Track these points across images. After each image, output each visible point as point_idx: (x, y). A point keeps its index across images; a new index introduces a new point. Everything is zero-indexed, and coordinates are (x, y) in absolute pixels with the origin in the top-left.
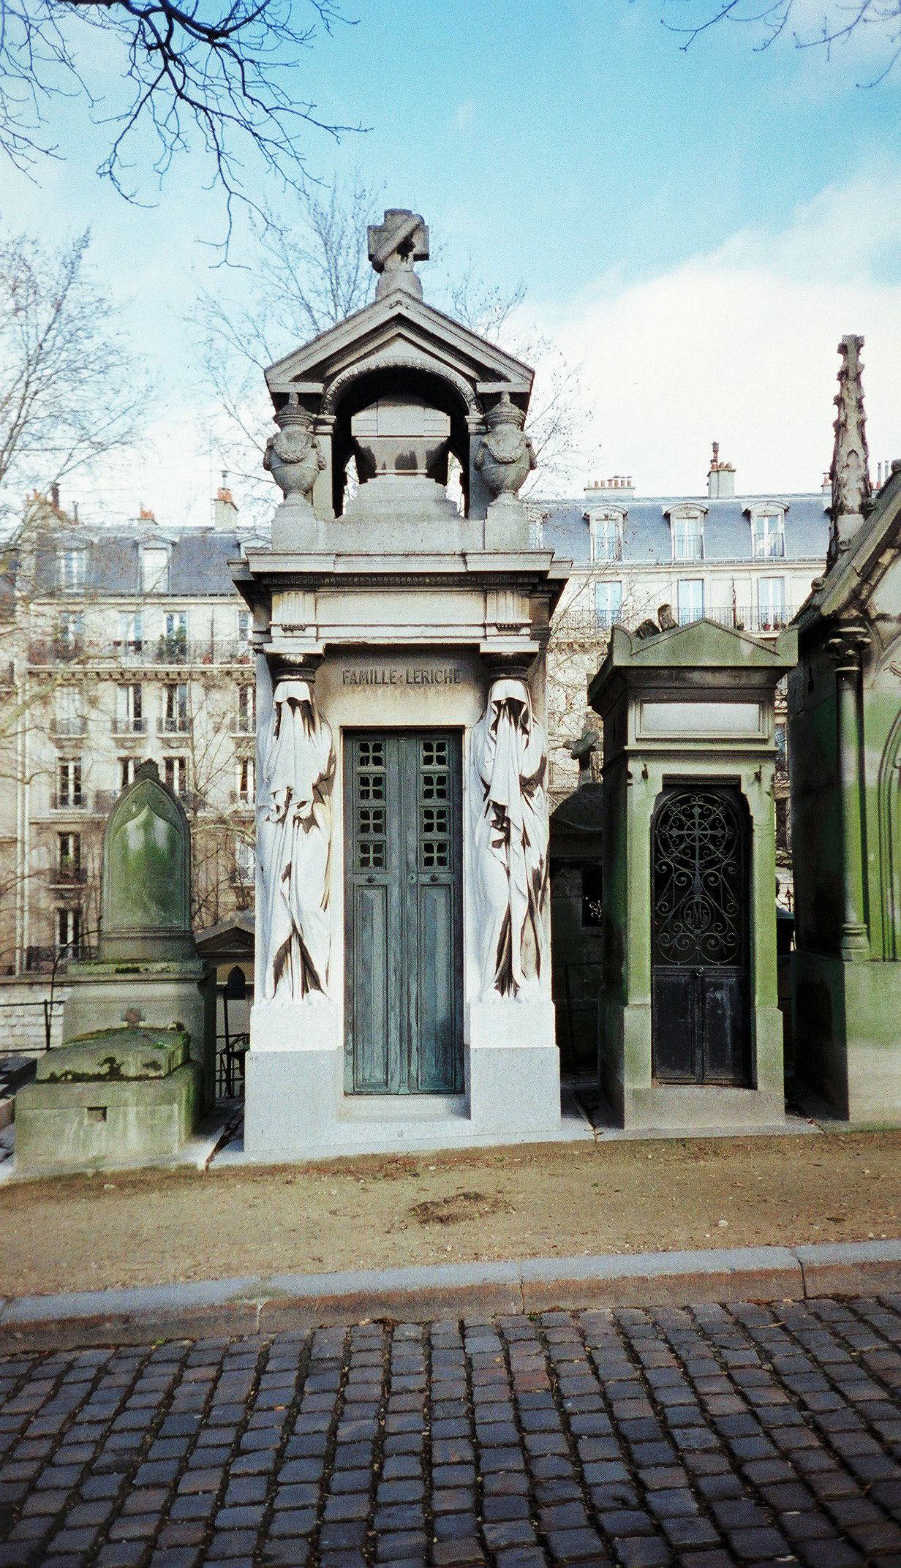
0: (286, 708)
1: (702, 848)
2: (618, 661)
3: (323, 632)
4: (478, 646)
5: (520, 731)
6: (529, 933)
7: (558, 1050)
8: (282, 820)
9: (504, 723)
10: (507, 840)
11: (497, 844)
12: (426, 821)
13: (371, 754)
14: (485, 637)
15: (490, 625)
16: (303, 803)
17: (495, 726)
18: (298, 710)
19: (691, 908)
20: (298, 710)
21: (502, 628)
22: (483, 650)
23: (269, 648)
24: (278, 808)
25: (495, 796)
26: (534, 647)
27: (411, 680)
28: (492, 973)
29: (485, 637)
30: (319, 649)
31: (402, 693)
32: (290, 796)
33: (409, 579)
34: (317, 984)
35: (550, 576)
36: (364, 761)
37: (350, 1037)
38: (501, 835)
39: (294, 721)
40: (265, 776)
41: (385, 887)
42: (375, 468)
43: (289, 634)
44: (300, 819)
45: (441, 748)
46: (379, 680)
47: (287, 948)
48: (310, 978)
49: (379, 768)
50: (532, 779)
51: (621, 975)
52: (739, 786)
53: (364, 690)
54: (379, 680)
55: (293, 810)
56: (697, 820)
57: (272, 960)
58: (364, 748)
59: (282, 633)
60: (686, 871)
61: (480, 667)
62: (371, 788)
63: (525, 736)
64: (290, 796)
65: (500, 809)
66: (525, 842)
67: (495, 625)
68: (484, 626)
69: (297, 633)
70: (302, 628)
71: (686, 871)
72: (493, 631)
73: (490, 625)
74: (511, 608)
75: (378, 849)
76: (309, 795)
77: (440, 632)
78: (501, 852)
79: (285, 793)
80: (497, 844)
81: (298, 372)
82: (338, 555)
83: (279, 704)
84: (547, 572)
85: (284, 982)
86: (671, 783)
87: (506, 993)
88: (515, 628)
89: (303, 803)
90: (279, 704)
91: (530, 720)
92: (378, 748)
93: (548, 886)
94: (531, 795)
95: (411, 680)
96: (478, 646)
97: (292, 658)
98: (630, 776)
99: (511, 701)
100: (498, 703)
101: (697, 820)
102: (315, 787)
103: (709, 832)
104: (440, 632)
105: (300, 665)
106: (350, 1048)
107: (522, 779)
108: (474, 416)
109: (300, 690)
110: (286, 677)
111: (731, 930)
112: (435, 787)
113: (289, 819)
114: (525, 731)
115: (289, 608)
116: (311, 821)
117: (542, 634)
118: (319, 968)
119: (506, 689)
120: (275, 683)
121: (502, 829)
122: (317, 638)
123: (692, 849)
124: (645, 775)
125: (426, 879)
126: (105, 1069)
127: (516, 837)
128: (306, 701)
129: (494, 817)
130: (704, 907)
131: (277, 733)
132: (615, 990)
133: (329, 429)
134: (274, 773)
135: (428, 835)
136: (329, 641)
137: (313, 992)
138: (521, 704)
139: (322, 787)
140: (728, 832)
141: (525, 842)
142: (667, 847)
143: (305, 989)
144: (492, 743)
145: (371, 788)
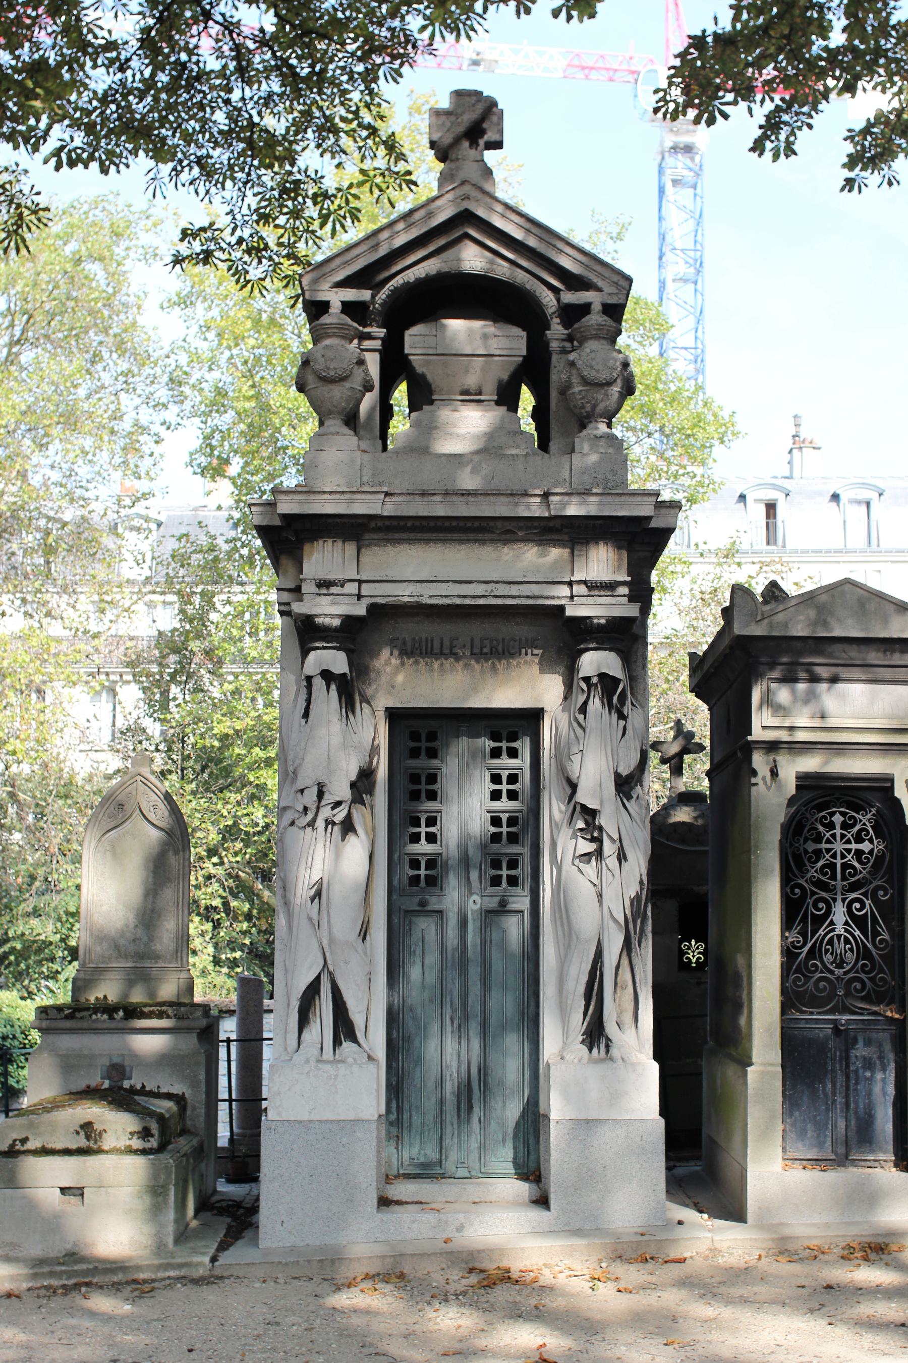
1: (845, 866)
2: (739, 629)
3: (366, 589)
4: (562, 608)
5: (615, 716)
7: (662, 1122)
8: (312, 824)
9: (595, 704)
10: (599, 853)
13: (424, 745)
14: (572, 597)
16: (338, 804)
17: (583, 709)
18: (333, 687)
19: (831, 942)
20: (333, 687)
21: (592, 586)
22: (569, 612)
23: (297, 608)
24: (306, 809)
25: (582, 797)
26: (633, 611)
27: (476, 651)
29: (572, 597)
32: (320, 795)
33: (476, 524)
34: (355, 1040)
35: (653, 524)
36: (415, 753)
37: (394, 1105)
38: (590, 847)
39: (327, 701)
40: (291, 769)
41: (440, 912)
42: (431, 392)
43: (324, 591)
44: (334, 824)
45: (513, 737)
46: (436, 649)
47: (313, 989)
48: (344, 1028)
50: (630, 776)
51: (736, 1028)
52: (892, 788)
54: (436, 649)
55: (326, 812)
56: (838, 831)
57: (295, 1004)
58: (415, 736)
59: (315, 590)
60: (824, 894)
61: (563, 638)
62: (423, 787)
63: (622, 723)
64: (320, 795)
65: (590, 814)
66: (622, 857)
67: (585, 582)
68: (570, 584)
69: (334, 590)
71: (824, 894)
72: (583, 589)
73: (579, 582)
74: (602, 562)
76: (345, 793)
77: (514, 590)
78: (590, 870)
79: (315, 789)
81: (340, 276)
82: (387, 494)
83: (309, 679)
84: (649, 519)
85: (312, 1034)
86: (806, 782)
87: (595, 1050)
88: (610, 587)
89: (338, 804)
91: (628, 703)
92: (432, 736)
93: (649, 913)
94: (629, 798)
95: (476, 651)
96: (562, 608)
97: (327, 621)
98: (754, 773)
99: (602, 676)
100: (587, 679)
101: (838, 831)
102: (353, 785)
103: (854, 846)
104: (514, 590)
105: (336, 630)
106: (393, 1117)
107: (617, 775)
108: (556, 330)
109: (338, 662)
110: (320, 644)
111: (881, 971)
112: (504, 787)
113: (320, 823)
114: (622, 716)
115: (324, 559)
116: (348, 827)
117: (642, 593)
118: (357, 1018)
119: (594, 661)
120: (305, 653)
121: (593, 839)
122: (359, 597)
123: (832, 866)
124: (774, 773)
126: (82, 1142)
127: (609, 848)
128: (345, 674)
129: (581, 824)
130: (847, 941)
131: (306, 715)
132: (733, 1045)
133: (377, 344)
134: (300, 765)
136: (374, 600)
137: (347, 1046)
138: (616, 681)
139: (363, 783)
140: (878, 846)
141: (622, 857)
142: (800, 865)
143: (337, 1042)
144: (579, 731)
145: (423, 787)
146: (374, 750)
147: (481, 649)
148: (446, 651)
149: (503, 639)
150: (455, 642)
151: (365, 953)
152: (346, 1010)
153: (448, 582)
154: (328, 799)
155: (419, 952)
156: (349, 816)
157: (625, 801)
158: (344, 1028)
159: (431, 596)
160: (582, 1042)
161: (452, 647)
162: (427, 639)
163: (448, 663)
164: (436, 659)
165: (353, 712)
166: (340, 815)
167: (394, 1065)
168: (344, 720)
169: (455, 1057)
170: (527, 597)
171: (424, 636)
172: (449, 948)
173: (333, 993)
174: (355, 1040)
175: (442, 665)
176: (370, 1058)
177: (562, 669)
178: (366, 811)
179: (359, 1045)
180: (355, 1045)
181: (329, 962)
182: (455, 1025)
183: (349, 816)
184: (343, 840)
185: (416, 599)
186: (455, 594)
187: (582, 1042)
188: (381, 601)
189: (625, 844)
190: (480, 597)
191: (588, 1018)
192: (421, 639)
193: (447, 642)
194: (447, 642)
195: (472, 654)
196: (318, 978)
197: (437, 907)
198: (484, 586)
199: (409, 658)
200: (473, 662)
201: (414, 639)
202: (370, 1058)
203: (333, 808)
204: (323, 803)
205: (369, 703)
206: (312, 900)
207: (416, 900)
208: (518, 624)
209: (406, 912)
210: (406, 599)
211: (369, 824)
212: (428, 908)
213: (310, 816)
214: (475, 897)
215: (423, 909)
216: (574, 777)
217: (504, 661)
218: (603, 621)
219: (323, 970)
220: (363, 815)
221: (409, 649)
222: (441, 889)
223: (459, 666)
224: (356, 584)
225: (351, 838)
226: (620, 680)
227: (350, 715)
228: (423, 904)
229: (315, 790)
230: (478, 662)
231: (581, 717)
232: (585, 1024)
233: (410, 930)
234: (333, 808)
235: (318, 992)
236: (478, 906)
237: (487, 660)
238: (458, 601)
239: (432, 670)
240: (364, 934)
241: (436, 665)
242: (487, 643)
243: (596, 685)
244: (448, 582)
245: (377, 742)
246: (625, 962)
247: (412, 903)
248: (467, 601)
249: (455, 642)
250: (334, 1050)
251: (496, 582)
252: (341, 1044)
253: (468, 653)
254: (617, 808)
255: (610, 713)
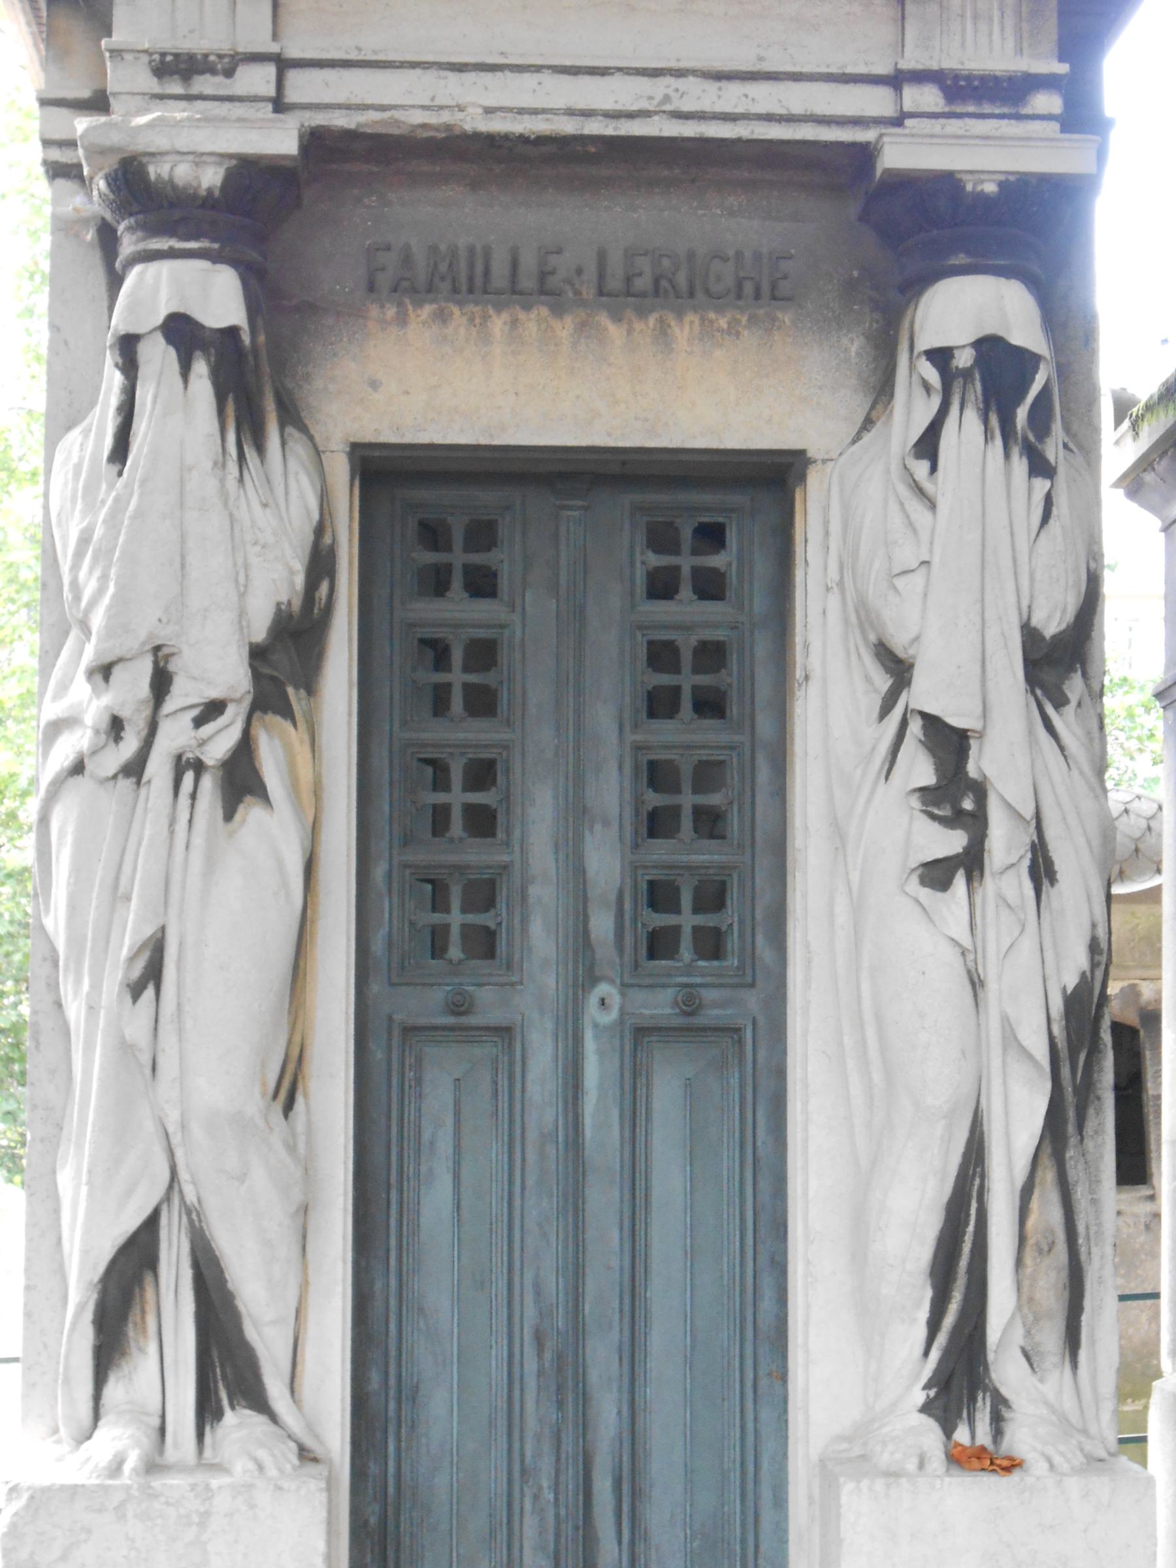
0: (157, 356)
3: (301, 86)
4: (865, 154)
5: (1020, 465)
6: (1047, 1211)
8: (135, 769)
9: (965, 433)
10: (972, 862)
11: (937, 874)
12: (654, 799)
15: (920, 77)
16: (213, 709)
17: (928, 445)
20: (201, 368)
27: (615, 283)
28: (907, 1358)
30: (281, 141)
31: (582, 326)
32: (161, 683)
34: (259, 1403)
38: (953, 842)
39: (182, 411)
41: (504, 1033)
43: (177, 88)
44: (199, 767)
48: (228, 1371)
49: (481, 610)
53: (442, 317)
55: (177, 733)
58: (433, 534)
64: (161, 683)
65: (949, 743)
66: (1042, 870)
70: (231, 64)
72: (927, 97)
73: (920, 77)
75: (484, 893)
77: (732, 97)
80: (937, 874)
89: (213, 709)
90: (128, 346)
92: (483, 534)
94: (1060, 702)
100: (941, 357)
104: (732, 97)
107: (1030, 634)
113: (158, 768)
114: (1040, 467)
116: (240, 781)
118: (266, 1336)
125: (658, 1005)
127: (1004, 843)
135: (661, 851)
137: (237, 1423)
138: (1025, 361)
139: (284, 659)
141: (1042, 870)
143: (207, 1411)
144: (917, 509)
146: (320, 564)
147: (628, 280)
148: (527, 282)
149: (691, 255)
150: (553, 260)
151: (291, 1148)
152: (235, 1318)
153: (538, 69)
154: (186, 692)
155: (445, 1146)
156: (245, 748)
157: (1050, 710)
158: (228, 1371)
159: (489, 111)
160: (926, 1409)
161: (544, 275)
162: (471, 250)
163: (533, 320)
164: (499, 308)
165: (260, 448)
166: (220, 742)
167: (373, 1468)
168: (233, 467)
169: (547, 1447)
170: (769, 118)
171: (462, 242)
172: (532, 1135)
173: (196, 1266)
174: (259, 1403)
175: (514, 323)
176: (306, 1455)
177: (854, 345)
178: (297, 737)
179: (273, 1418)
180: (260, 1419)
181: (183, 1175)
182: (548, 1355)
183: (245, 748)
184: (229, 816)
185: (445, 117)
186: (560, 103)
187: (926, 1409)
188: (341, 121)
189: (1052, 833)
190: (631, 115)
191: (942, 1339)
192: (453, 252)
193: (529, 261)
194: (529, 261)
195: (601, 293)
196: (152, 1223)
197: (494, 1017)
198: (644, 84)
199: (419, 304)
200: (604, 319)
201: (434, 249)
202: (306, 1455)
203: (199, 722)
204: (169, 706)
205: (304, 429)
206: (136, 990)
207: (438, 996)
208: (732, 214)
209: (409, 1031)
210: (417, 118)
211: (305, 773)
212: (472, 1020)
213: (130, 745)
214: (603, 989)
215: (460, 1025)
216: (899, 642)
217: (691, 317)
218: (990, 188)
219: (167, 1198)
220: (288, 748)
221: (422, 278)
222: (509, 966)
223: (564, 328)
224: (271, 70)
225: (252, 813)
226: (1036, 359)
227: (250, 453)
228: (460, 1006)
229: (144, 669)
230: (617, 318)
231: (921, 468)
232: (935, 1354)
233: (419, 1081)
234: (199, 722)
235: (151, 1263)
236: (614, 1014)
237: (642, 313)
238: (568, 127)
239: (486, 338)
240: (288, 1091)
241: (498, 323)
242: (644, 264)
243: (967, 374)
244: (538, 69)
245: (327, 540)
246: (1048, 1176)
247: (425, 1004)
248: (595, 127)
249: (553, 260)
250: (200, 1436)
251: (680, 73)
252: (218, 1415)
253: (589, 292)
254: (1031, 732)
255: (1007, 455)
